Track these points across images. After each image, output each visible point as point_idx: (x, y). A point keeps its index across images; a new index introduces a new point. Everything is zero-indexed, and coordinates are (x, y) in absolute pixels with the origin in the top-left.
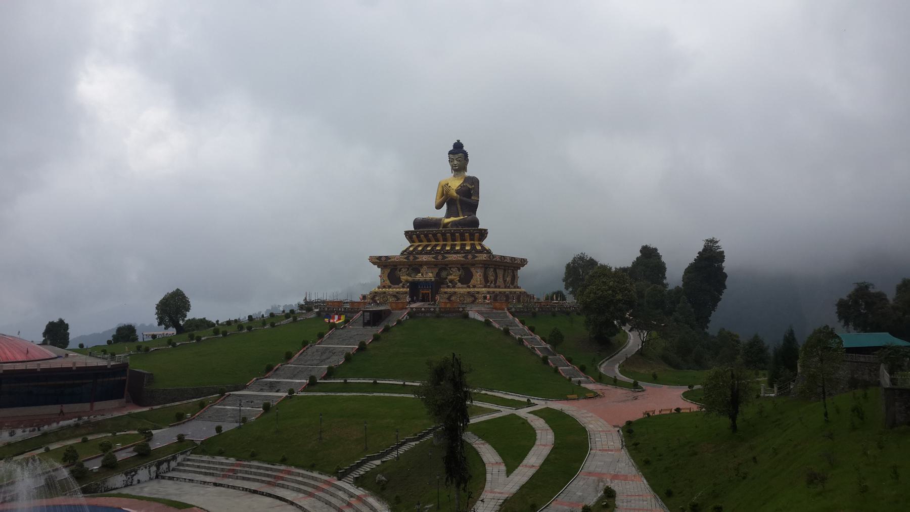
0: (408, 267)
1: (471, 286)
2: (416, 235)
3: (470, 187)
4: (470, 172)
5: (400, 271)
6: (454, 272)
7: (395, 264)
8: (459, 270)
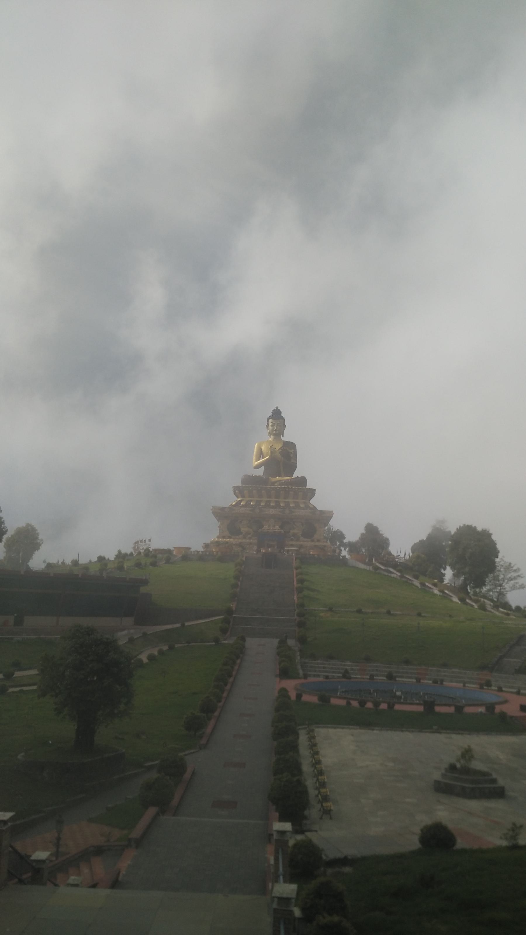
4: (287, 437)
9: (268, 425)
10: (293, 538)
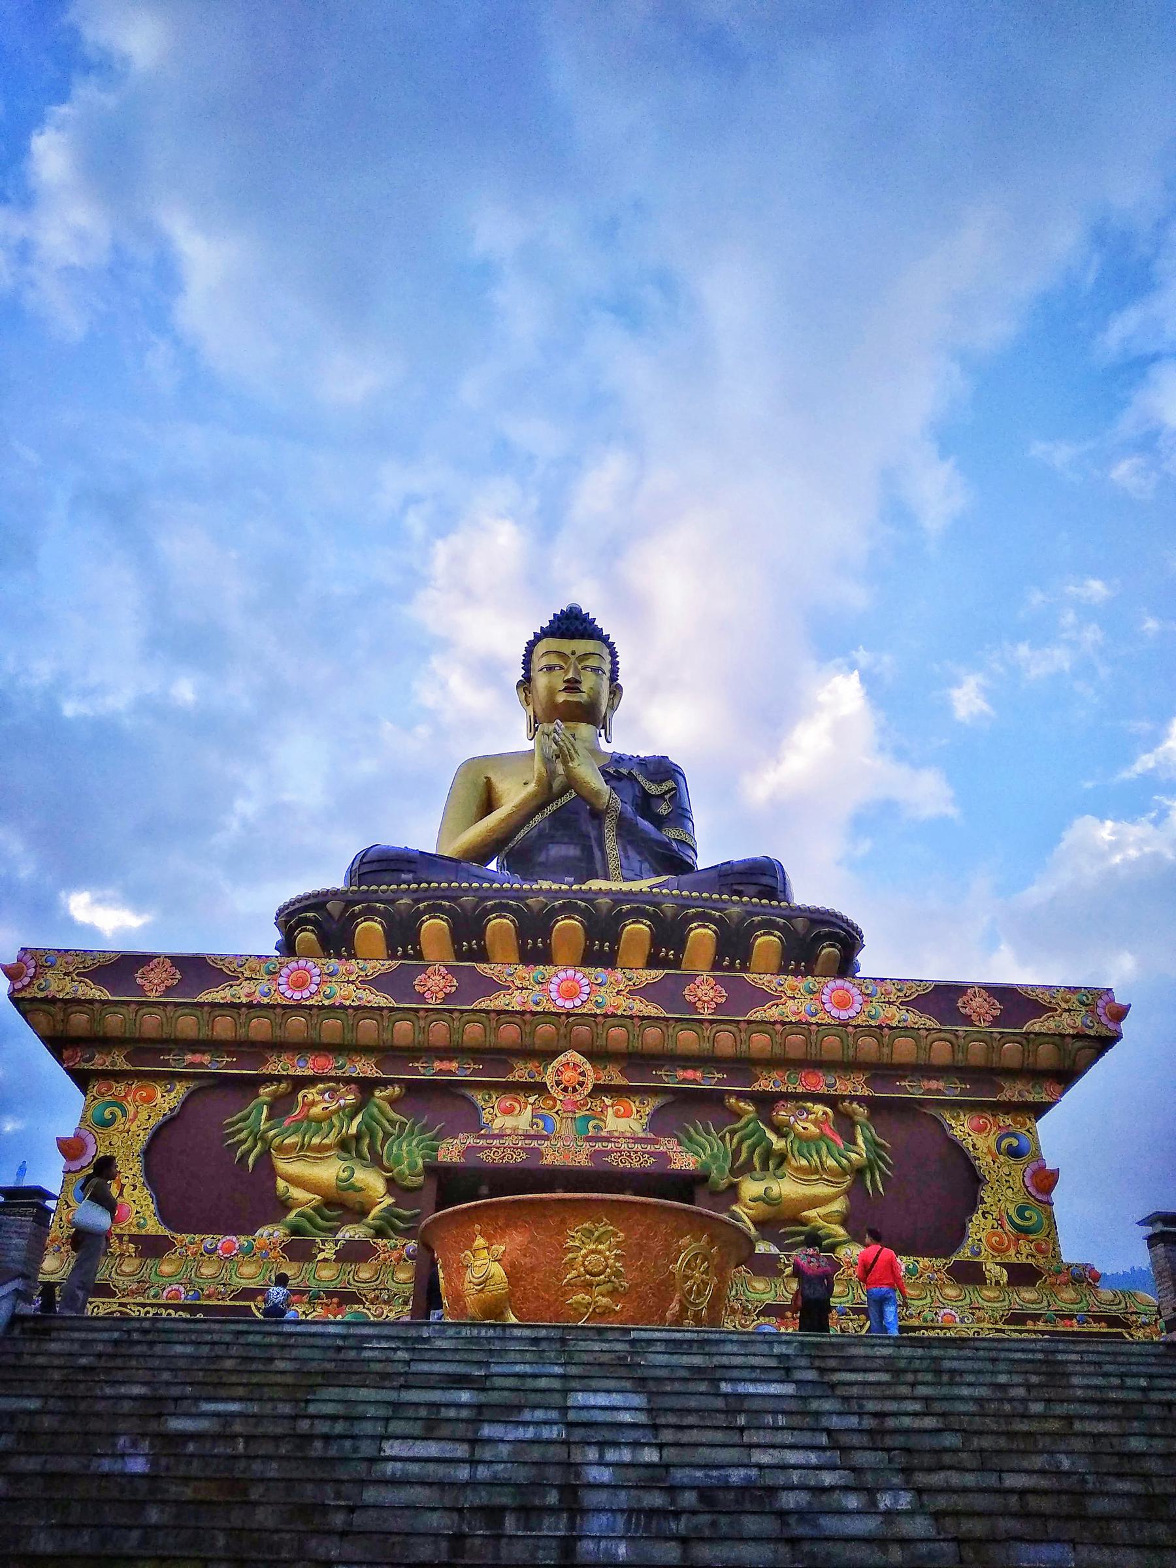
0: (364, 1068)
1: (994, 1270)
2: (383, 915)
3: (654, 789)
5: (280, 1107)
6: (805, 1140)
7: (260, 1028)
8: (845, 1125)
9: (526, 683)
10: (774, 1250)
